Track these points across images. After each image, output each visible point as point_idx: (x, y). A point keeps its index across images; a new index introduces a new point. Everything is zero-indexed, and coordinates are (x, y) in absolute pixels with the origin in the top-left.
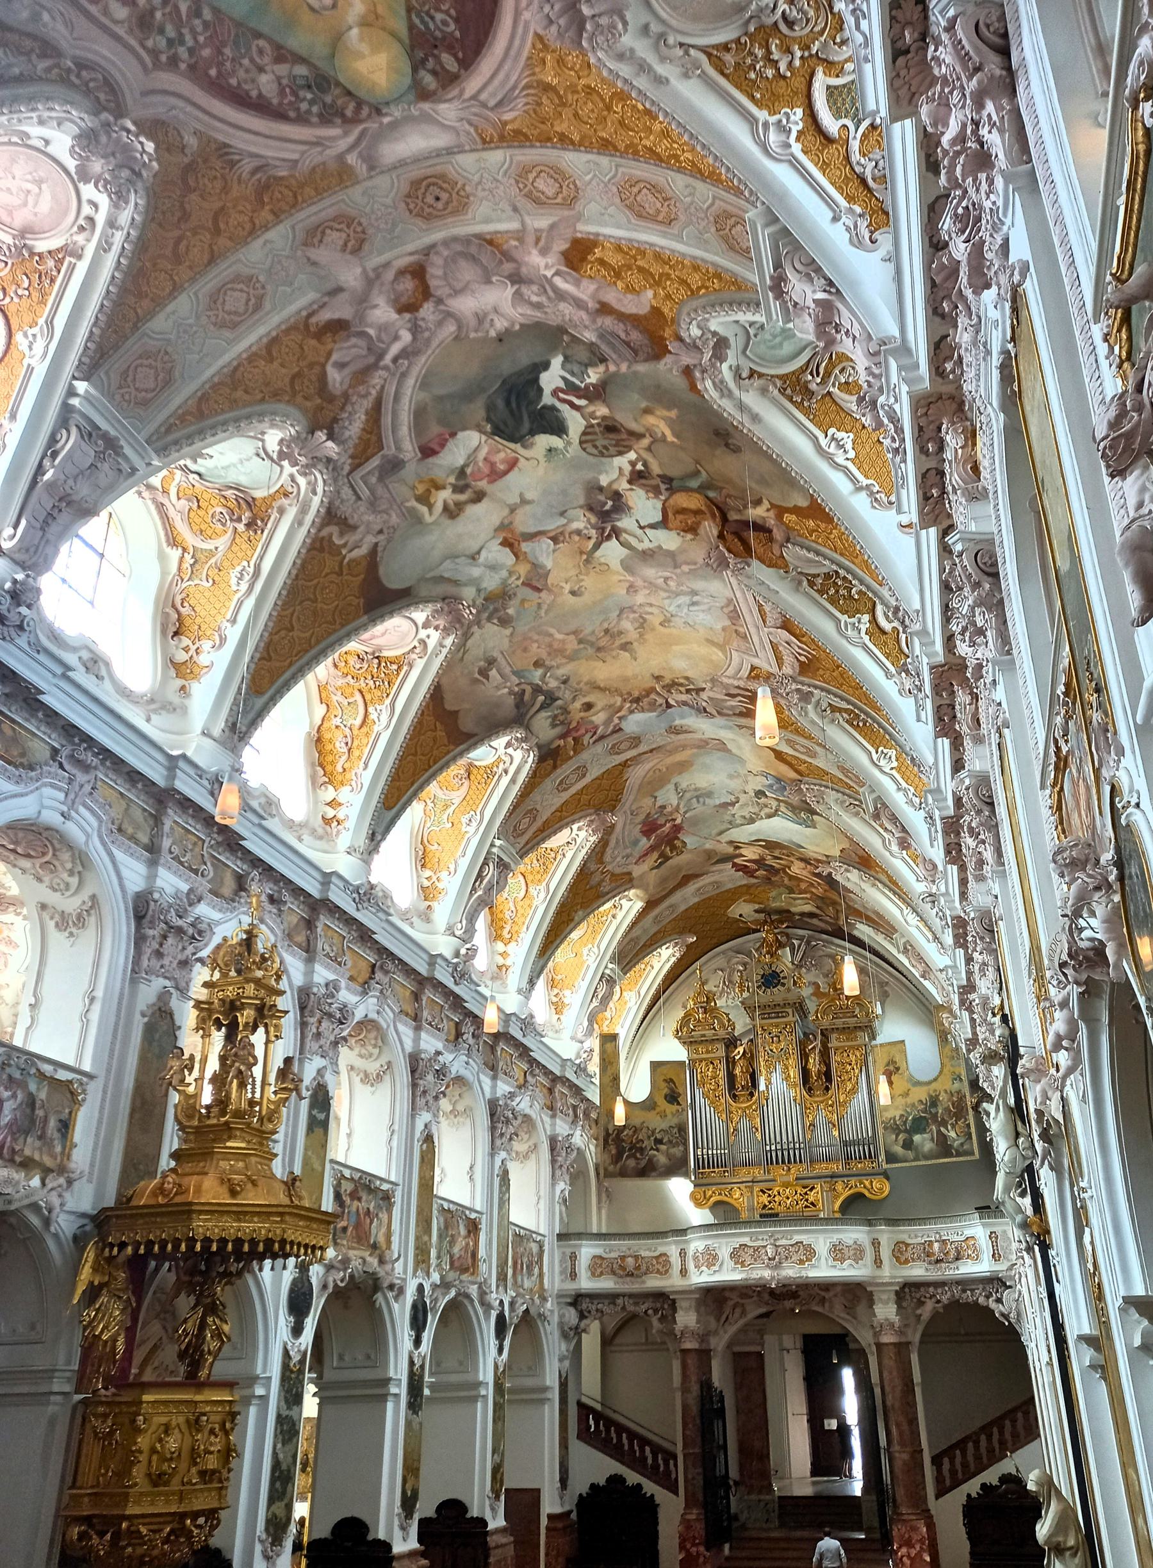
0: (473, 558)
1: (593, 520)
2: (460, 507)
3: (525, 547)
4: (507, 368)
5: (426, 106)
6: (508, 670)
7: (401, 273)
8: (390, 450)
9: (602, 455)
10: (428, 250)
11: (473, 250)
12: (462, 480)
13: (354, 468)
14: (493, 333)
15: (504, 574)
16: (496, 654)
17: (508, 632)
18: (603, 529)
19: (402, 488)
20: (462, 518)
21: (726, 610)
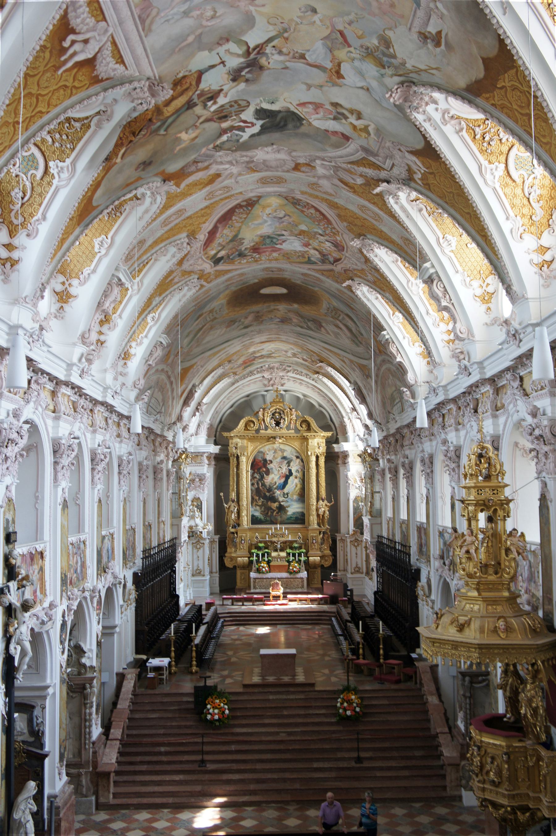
0: (368, 89)
1: (263, 61)
2: (352, 112)
3: (329, 65)
4: (276, 136)
5: (259, 195)
6: (421, 13)
7: (303, 172)
8: (360, 155)
9: (236, 102)
10: (288, 171)
11: (266, 168)
12: (339, 117)
13: (384, 169)
14: (274, 146)
15: (357, 63)
16: (415, 36)
17: (390, 34)
18: (258, 53)
19: (372, 143)
20: (355, 107)
21: (154, 12)
